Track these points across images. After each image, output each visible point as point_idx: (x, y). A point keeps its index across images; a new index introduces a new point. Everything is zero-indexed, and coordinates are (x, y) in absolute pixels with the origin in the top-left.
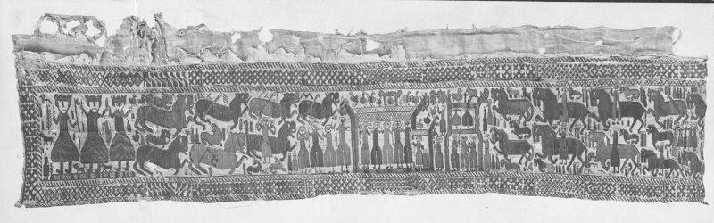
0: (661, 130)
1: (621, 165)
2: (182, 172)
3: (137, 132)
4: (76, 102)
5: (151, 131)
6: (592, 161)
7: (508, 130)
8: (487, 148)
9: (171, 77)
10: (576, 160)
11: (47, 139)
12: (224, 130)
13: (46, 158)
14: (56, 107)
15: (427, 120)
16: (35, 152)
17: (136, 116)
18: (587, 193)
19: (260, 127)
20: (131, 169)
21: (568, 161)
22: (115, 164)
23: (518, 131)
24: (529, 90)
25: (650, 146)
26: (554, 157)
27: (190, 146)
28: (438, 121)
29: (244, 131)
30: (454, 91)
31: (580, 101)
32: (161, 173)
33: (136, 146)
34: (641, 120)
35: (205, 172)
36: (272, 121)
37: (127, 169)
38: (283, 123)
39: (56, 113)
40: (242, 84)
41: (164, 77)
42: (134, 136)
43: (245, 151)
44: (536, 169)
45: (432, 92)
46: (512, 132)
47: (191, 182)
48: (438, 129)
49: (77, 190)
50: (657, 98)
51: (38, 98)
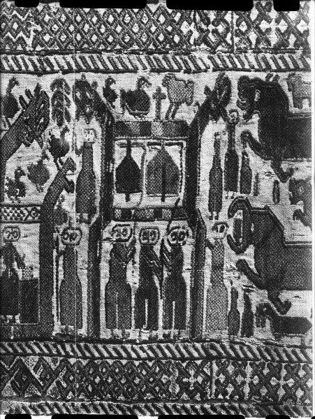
8: (217, 267)
15: (38, 173)
28: (73, 178)
30: (125, 83)
45: (58, 83)
48: (68, 202)
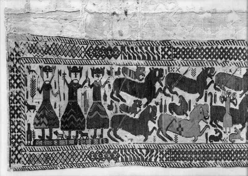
2: (150, 138)
3: (112, 102)
4: (60, 73)
5: (124, 101)
9: (145, 51)
11: (31, 108)
12: (190, 101)
13: (29, 125)
14: (41, 79)
16: (19, 119)
17: (112, 86)
19: (224, 99)
20: (105, 136)
22: (91, 132)
27: (158, 114)
29: (208, 102)
32: (132, 140)
33: (110, 114)
35: (171, 139)
36: (234, 94)
37: (101, 136)
38: (244, 96)
39: (40, 85)
40: (209, 59)
41: (139, 50)
42: (108, 106)
43: (209, 121)
47: (159, 148)
49: (58, 155)
51: (26, 69)
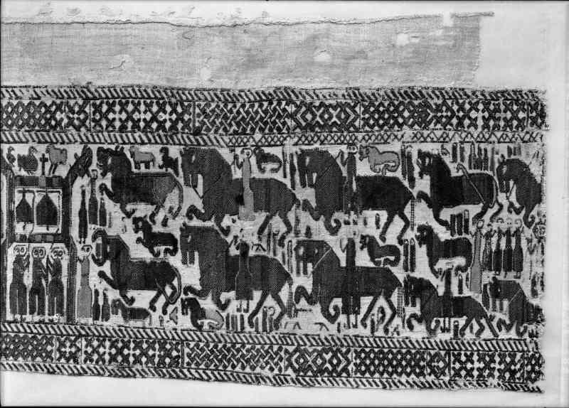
0: (443, 234)
1: (364, 310)
6: (303, 303)
7: (130, 238)
8: (85, 275)
10: (270, 301)
18: (290, 371)
21: (253, 305)
23: (150, 240)
24: (174, 152)
25: (422, 270)
26: (224, 296)
30: (21, 150)
31: (278, 176)
34: (403, 217)
44: (185, 322)
46: (139, 240)
50: (435, 168)
